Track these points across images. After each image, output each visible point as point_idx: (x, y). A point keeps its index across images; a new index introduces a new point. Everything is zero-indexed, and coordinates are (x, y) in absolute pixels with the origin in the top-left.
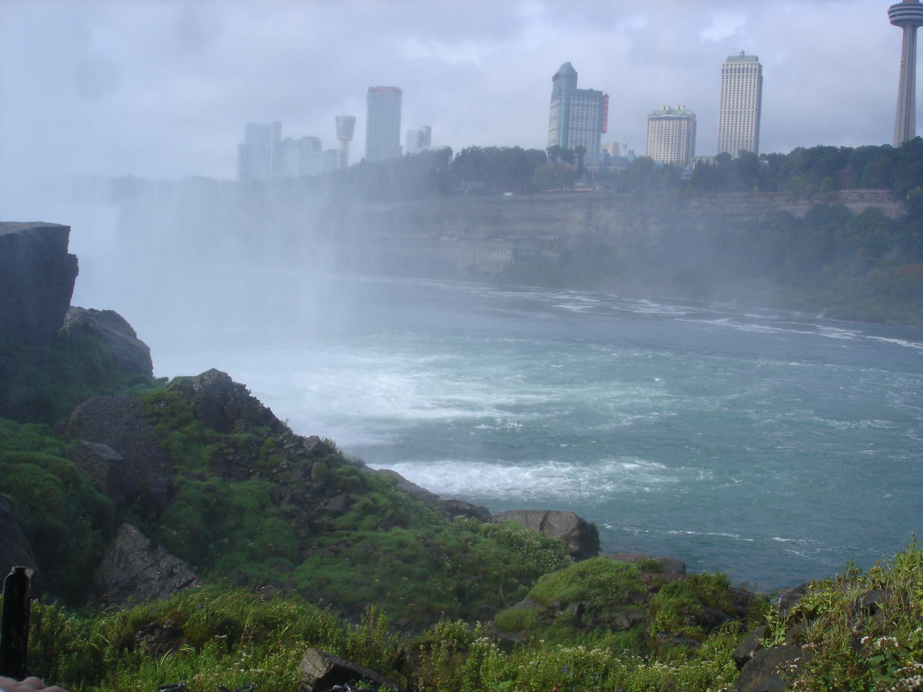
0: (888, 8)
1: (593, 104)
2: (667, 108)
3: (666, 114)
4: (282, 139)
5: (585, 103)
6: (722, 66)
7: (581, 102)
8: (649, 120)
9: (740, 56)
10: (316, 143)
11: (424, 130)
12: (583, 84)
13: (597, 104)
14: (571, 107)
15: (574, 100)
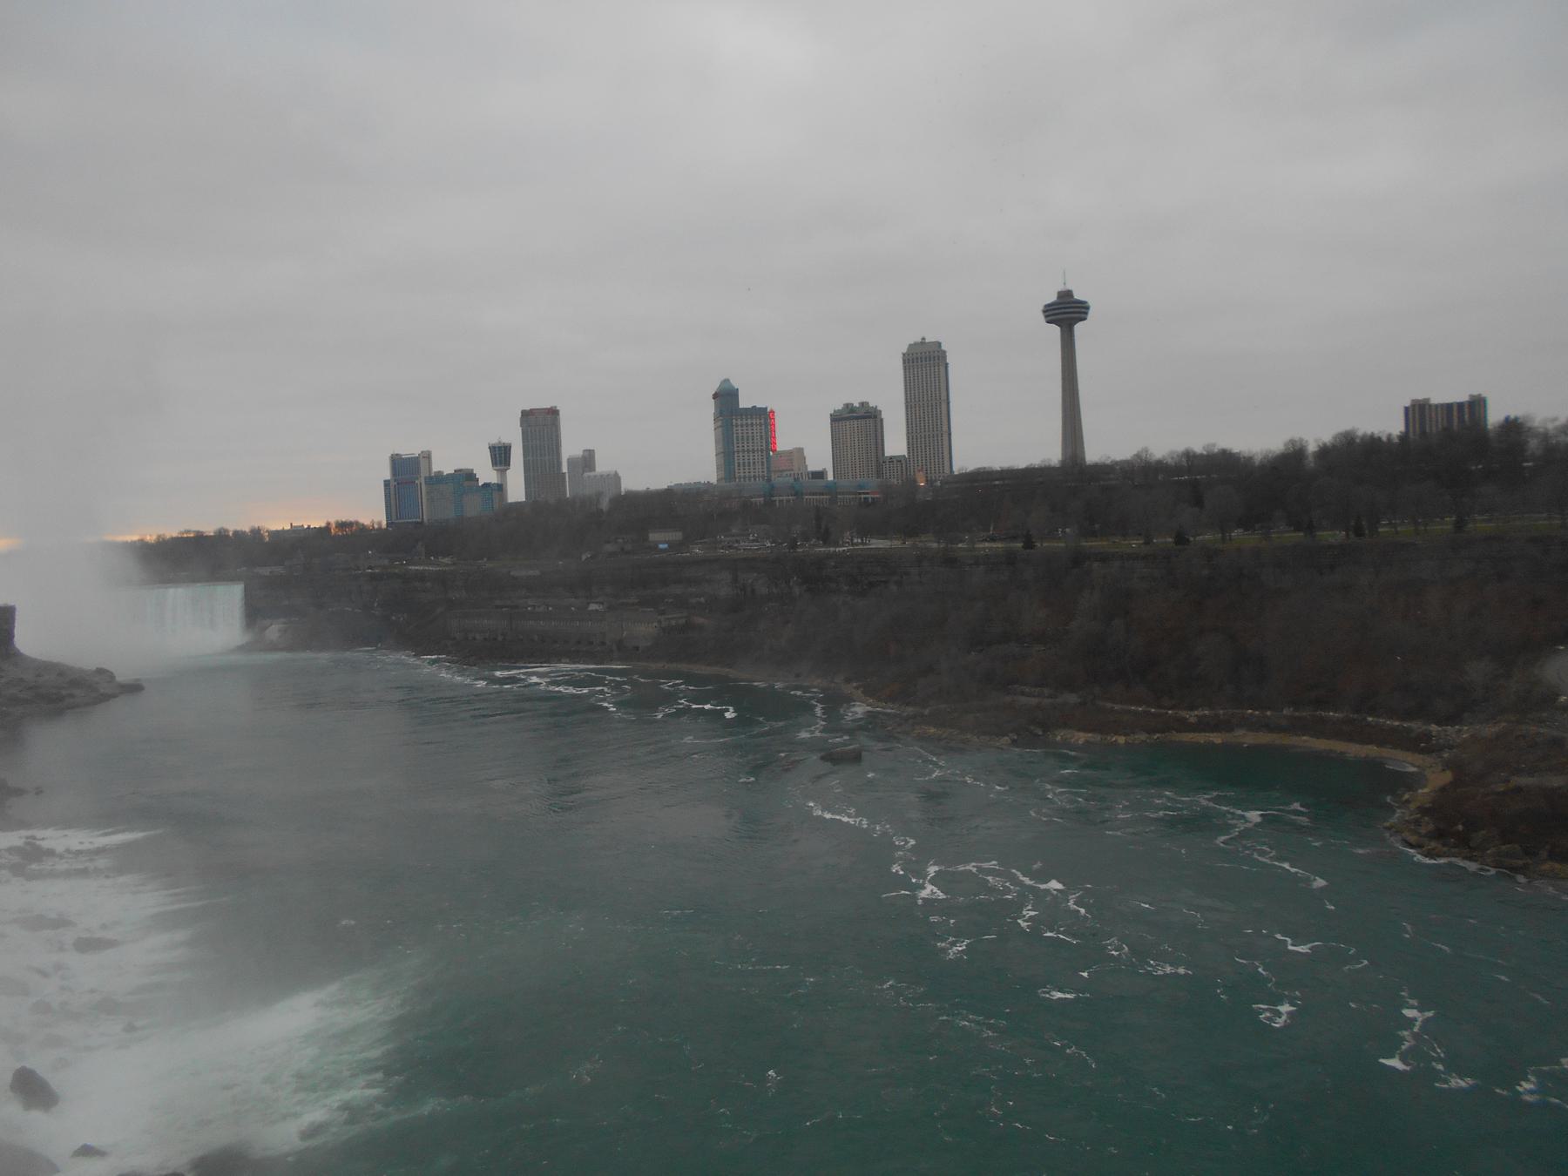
0: (1042, 308)
1: (758, 422)
2: (850, 407)
3: (849, 413)
4: (433, 475)
5: (749, 421)
6: (902, 356)
7: (744, 422)
8: (832, 421)
9: (921, 343)
10: (470, 476)
11: (587, 454)
12: (744, 403)
13: (762, 421)
14: (735, 429)
15: (736, 420)
